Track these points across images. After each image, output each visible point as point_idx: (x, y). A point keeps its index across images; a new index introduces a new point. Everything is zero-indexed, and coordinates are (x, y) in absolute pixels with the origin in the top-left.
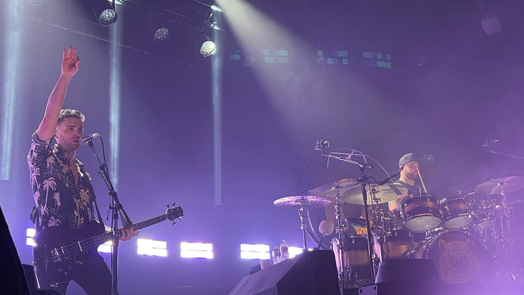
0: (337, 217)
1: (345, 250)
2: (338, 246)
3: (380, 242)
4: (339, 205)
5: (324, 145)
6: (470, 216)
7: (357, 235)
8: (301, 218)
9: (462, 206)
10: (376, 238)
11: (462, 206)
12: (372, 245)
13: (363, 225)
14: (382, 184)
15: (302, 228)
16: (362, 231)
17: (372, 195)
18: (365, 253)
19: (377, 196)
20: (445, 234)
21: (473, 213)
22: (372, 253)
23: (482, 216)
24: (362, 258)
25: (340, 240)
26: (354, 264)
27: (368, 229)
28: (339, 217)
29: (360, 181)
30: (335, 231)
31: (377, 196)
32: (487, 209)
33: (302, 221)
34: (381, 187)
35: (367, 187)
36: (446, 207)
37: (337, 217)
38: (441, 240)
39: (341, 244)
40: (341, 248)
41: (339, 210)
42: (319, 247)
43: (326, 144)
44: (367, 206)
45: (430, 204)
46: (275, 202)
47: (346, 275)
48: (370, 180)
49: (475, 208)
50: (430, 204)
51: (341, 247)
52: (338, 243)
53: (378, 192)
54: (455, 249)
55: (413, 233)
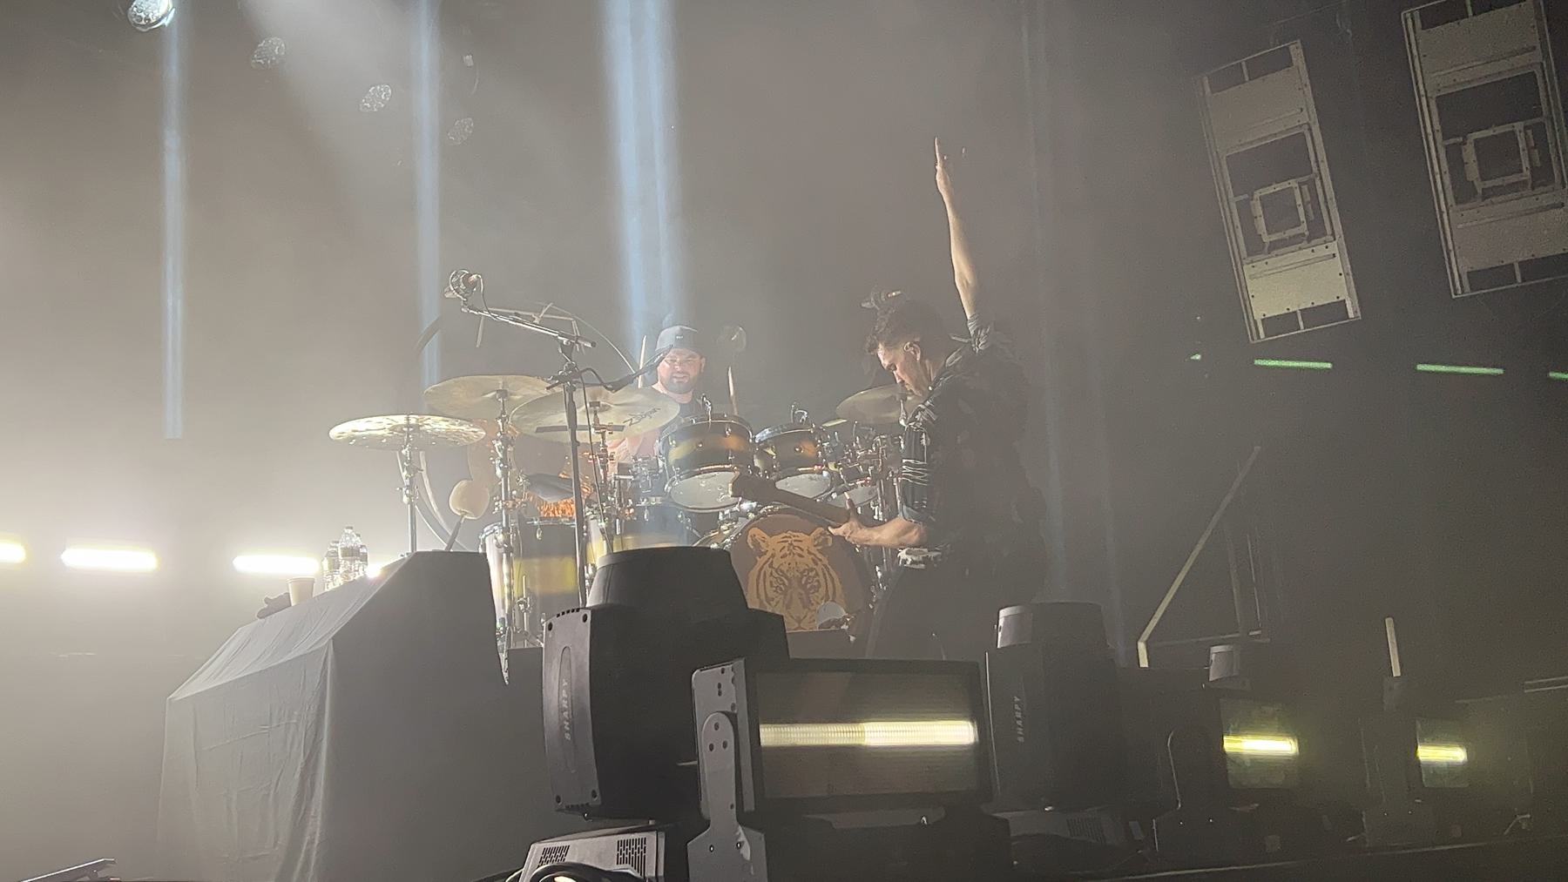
0: (499, 472)
1: (517, 556)
2: (498, 546)
3: (608, 534)
4: (507, 442)
5: (471, 286)
6: (825, 473)
7: (548, 518)
8: (405, 474)
9: (808, 449)
10: (596, 526)
11: (808, 449)
12: (585, 543)
13: (565, 493)
14: (616, 387)
15: (405, 499)
16: (560, 507)
17: (592, 417)
18: (569, 562)
19: (605, 419)
20: (764, 515)
21: (832, 467)
22: (584, 562)
23: (853, 475)
24: (564, 574)
25: (505, 531)
26: (537, 589)
27: (578, 499)
28: (505, 475)
29: (561, 380)
30: (491, 508)
31: (605, 419)
32: (866, 457)
33: (407, 482)
34: (614, 398)
35: (578, 396)
36: (770, 452)
37: (499, 472)
38: (755, 531)
39: (507, 541)
40: (508, 551)
41: (505, 453)
42: (450, 546)
43: (475, 284)
44: (575, 443)
45: (732, 442)
46: (334, 433)
47: (516, 618)
48: (588, 377)
49: (836, 457)
50: (732, 442)
51: (508, 551)
52: (501, 537)
53: (605, 409)
54: (786, 551)
55: (688, 515)
